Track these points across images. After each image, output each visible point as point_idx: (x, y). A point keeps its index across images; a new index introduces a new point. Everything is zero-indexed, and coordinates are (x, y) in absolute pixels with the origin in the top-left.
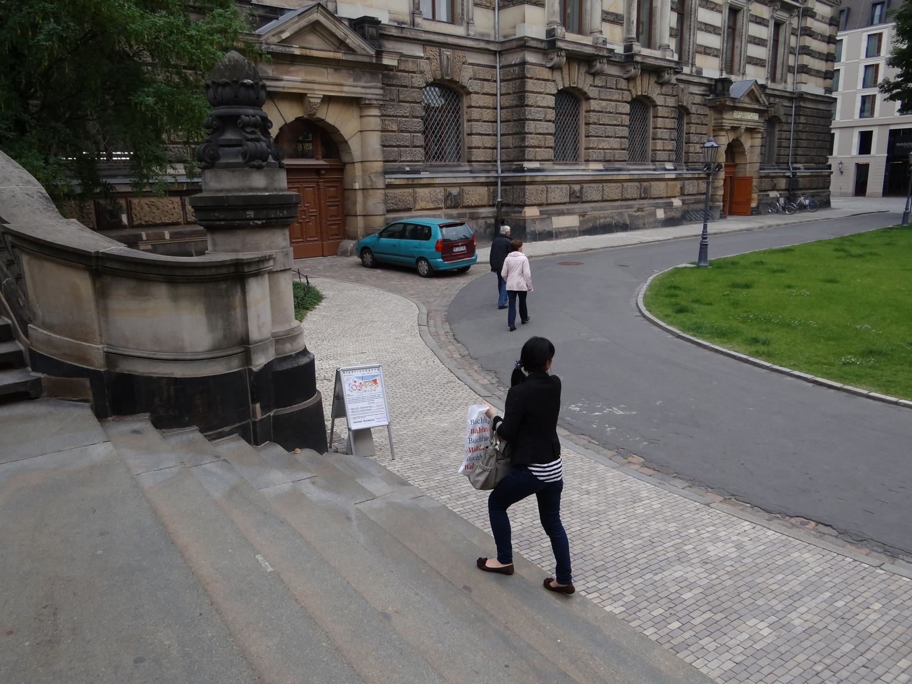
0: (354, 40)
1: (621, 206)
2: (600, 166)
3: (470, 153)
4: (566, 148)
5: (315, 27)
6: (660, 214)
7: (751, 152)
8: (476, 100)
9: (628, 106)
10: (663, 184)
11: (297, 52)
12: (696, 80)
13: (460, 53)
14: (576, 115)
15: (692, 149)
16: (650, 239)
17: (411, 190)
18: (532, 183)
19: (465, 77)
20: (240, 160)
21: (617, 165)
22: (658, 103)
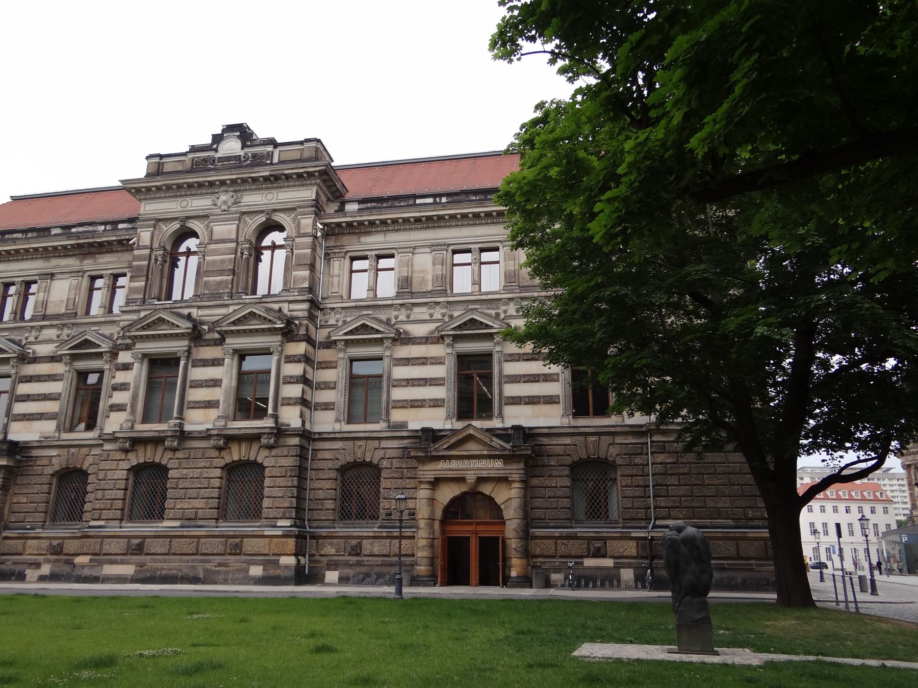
1: (193, 561)
2: (177, 524)
6: (256, 571)
21: (200, 523)
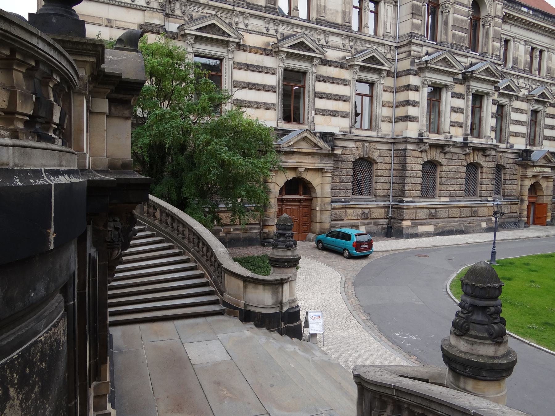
0: (321, 143)
1: (460, 221)
2: (447, 199)
3: (376, 192)
4: (428, 189)
5: (305, 139)
6: (484, 225)
7: (547, 189)
8: (380, 166)
9: (465, 168)
10: (485, 209)
11: (296, 150)
12: (510, 151)
13: (373, 144)
14: (435, 173)
15: (507, 188)
16: (473, 241)
17: (344, 210)
18: (407, 209)
19: (375, 155)
20: (284, 247)
21: (458, 199)
22: (483, 166)
